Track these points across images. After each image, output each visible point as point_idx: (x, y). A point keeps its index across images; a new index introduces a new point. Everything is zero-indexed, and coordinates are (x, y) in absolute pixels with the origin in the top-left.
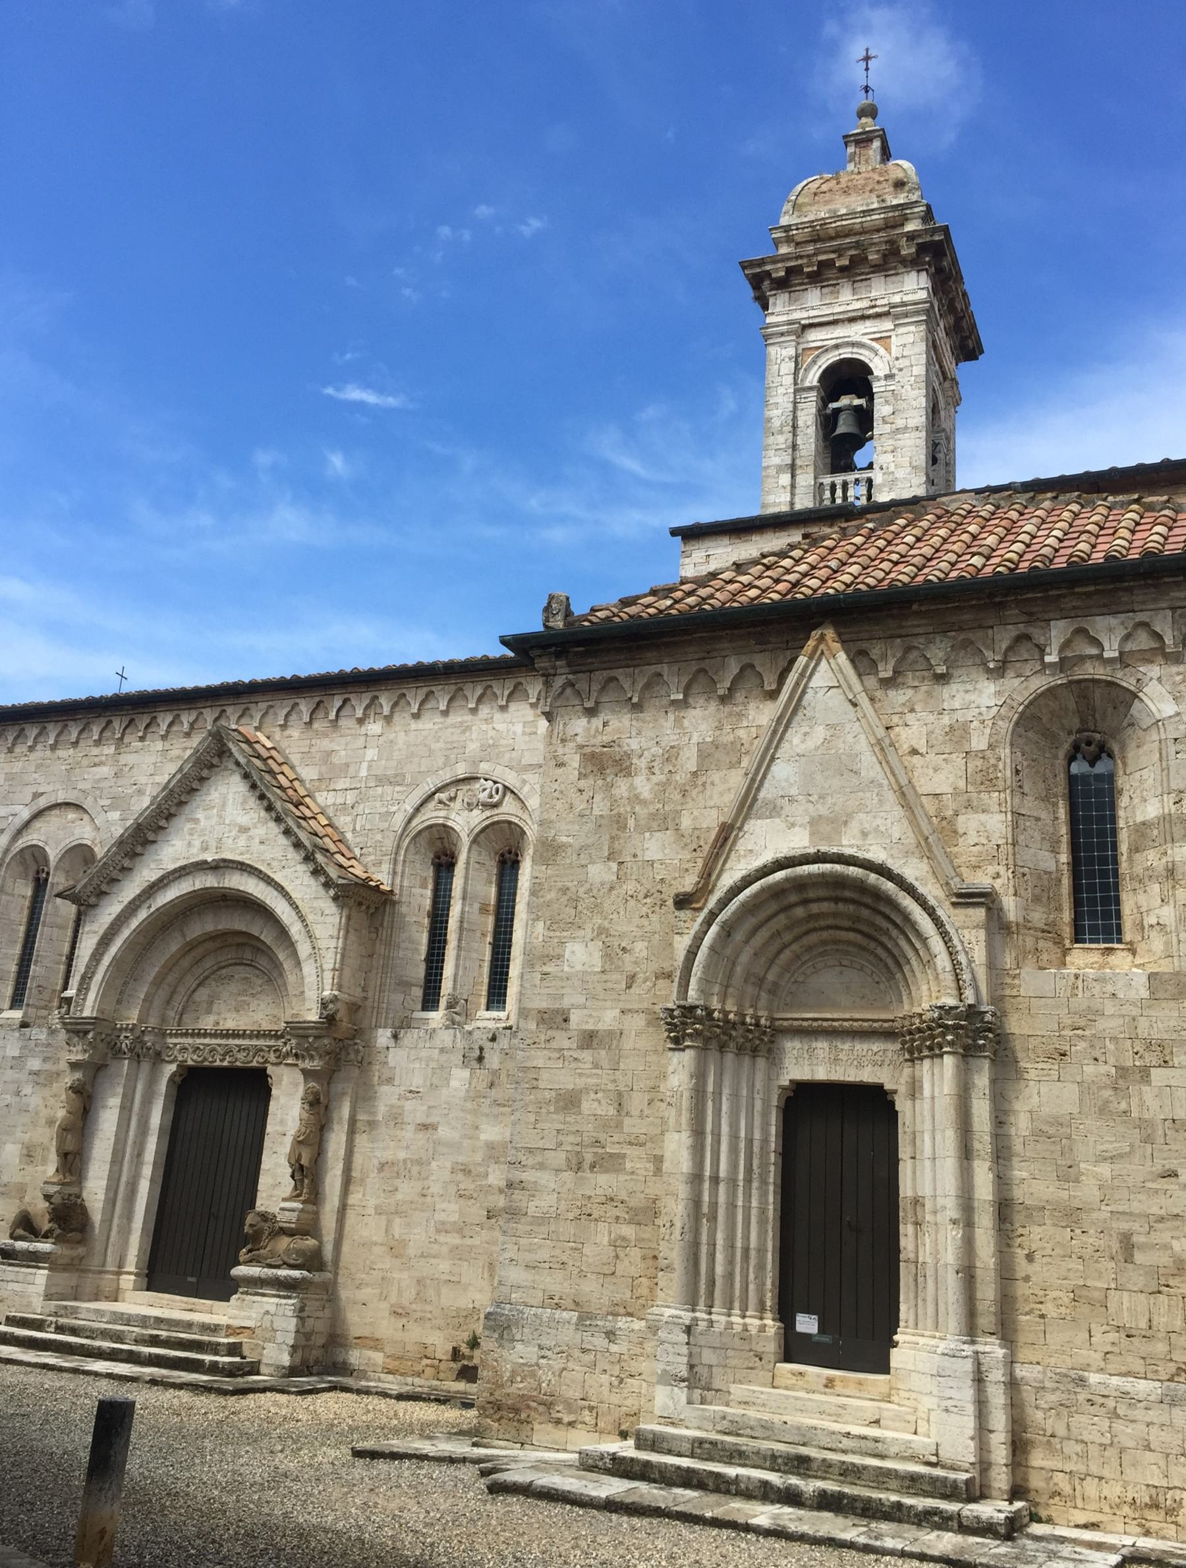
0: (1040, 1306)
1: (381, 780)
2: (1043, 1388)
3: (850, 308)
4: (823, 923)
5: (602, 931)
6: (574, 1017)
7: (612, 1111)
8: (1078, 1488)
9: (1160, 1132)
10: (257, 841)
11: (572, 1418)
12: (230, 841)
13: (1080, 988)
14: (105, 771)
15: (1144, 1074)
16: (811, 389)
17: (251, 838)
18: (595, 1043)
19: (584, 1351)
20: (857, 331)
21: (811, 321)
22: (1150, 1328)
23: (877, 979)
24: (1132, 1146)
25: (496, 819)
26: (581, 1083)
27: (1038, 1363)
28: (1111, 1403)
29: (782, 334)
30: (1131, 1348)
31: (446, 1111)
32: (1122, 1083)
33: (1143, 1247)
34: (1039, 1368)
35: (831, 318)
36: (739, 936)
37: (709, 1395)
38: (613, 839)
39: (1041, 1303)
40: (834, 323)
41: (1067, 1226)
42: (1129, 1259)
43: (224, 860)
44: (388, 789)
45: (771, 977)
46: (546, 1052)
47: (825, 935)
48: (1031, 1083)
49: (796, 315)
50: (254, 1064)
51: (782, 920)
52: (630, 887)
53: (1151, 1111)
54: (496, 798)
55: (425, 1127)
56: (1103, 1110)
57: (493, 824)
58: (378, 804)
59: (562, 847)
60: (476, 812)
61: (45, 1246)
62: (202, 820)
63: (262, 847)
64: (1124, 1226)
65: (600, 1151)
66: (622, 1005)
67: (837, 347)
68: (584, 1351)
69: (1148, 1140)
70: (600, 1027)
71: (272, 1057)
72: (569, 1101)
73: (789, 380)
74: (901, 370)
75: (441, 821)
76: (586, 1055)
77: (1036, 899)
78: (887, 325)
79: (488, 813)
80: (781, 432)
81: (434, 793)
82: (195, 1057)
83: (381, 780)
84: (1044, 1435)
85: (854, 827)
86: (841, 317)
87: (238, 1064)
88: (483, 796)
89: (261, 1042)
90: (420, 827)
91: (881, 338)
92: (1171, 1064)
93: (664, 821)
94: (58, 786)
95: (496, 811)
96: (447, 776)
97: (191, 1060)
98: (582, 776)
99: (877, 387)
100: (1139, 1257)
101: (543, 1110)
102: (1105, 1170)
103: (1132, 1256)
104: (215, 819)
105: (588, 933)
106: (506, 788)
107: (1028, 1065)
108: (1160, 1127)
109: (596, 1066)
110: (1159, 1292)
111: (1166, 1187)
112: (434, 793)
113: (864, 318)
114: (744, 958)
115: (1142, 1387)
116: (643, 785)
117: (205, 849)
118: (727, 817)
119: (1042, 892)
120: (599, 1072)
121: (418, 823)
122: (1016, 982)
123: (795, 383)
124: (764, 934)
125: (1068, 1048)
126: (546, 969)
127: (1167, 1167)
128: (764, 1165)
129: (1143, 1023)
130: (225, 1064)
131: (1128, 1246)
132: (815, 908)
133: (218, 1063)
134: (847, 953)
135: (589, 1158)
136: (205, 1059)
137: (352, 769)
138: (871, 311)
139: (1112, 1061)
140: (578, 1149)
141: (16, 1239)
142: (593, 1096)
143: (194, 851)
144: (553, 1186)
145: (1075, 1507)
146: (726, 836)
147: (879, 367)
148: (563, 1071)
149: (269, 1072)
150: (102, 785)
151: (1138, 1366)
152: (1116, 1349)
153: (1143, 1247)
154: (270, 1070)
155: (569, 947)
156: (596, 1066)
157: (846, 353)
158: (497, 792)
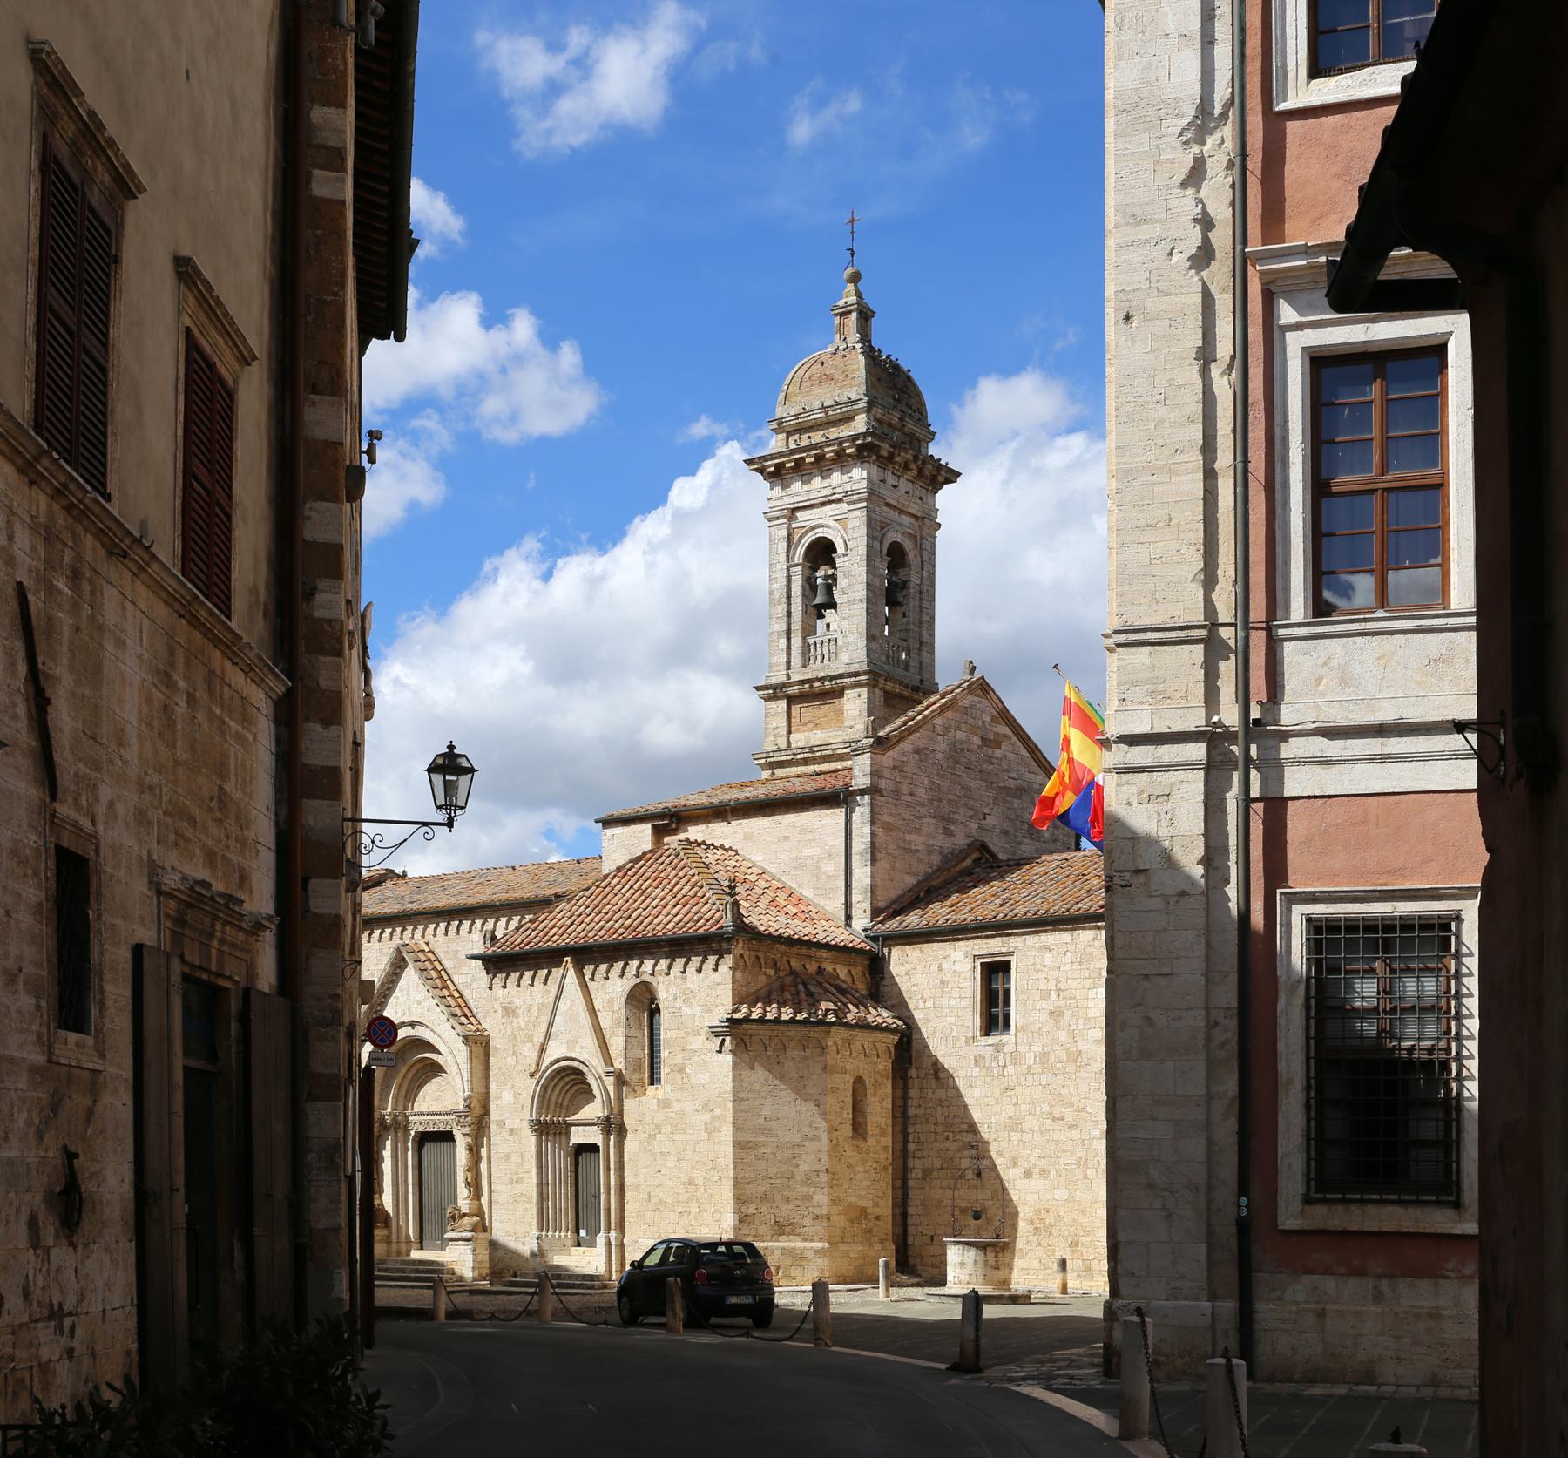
5: (513, 1086)
16: (797, 565)
20: (826, 514)
21: (797, 505)
29: (778, 518)
35: (808, 503)
36: (549, 1091)
38: (514, 1046)
40: (811, 507)
45: (565, 1104)
49: (787, 500)
51: (562, 1083)
52: (519, 1067)
56: (645, 1150)
67: (813, 528)
73: (783, 558)
76: (510, 1138)
77: (635, 1070)
80: (779, 603)
85: (578, 1046)
93: (529, 1038)
98: (503, 1017)
99: (839, 562)
102: (645, 1171)
105: (508, 1087)
114: (554, 1098)
116: (521, 1021)
118: (541, 1040)
119: (638, 1067)
123: (788, 562)
124: (558, 1088)
128: (566, 1177)
131: (650, 1197)
146: (543, 1049)
155: (504, 1093)
157: (819, 533)
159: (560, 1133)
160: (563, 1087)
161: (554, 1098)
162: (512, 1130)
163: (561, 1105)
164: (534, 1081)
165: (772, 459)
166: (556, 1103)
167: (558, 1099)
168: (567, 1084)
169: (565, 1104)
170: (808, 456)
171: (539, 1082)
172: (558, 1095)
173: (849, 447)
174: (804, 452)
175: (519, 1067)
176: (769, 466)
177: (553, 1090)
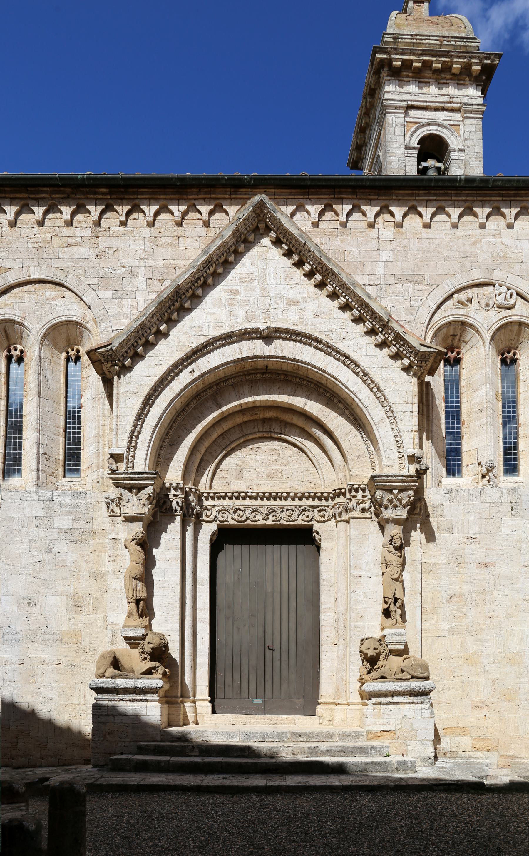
1: (399, 280)
3: (437, 99)
10: (310, 314)
12: (279, 312)
14: (83, 251)
25: (511, 319)
31: (501, 552)
43: (277, 330)
44: (408, 287)
50: (299, 522)
54: (512, 302)
55: (485, 565)
57: (507, 324)
58: (401, 300)
60: (492, 312)
62: (242, 292)
63: (316, 319)
71: (316, 515)
74: (468, 147)
75: (461, 318)
78: (458, 116)
79: (505, 313)
81: (452, 295)
82: (235, 516)
83: (399, 280)
86: (431, 104)
87: (282, 522)
88: (500, 299)
89: (304, 503)
90: (442, 322)
91: (453, 125)
94: (27, 263)
95: (510, 312)
96: (465, 281)
97: (230, 519)
104: (257, 291)
106: (518, 294)
112: (452, 295)
113: (444, 109)
117: (251, 319)
121: (441, 319)
130: (269, 522)
133: (261, 522)
136: (248, 519)
137: (368, 269)
138: (450, 105)
143: (240, 320)
147: (453, 142)
149: (315, 529)
150: (84, 264)
154: (317, 527)
158: (511, 296)
165: (402, 54)
170: (437, 61)
173: (477, 64)
174: (433, 56)
176: (396, 60)
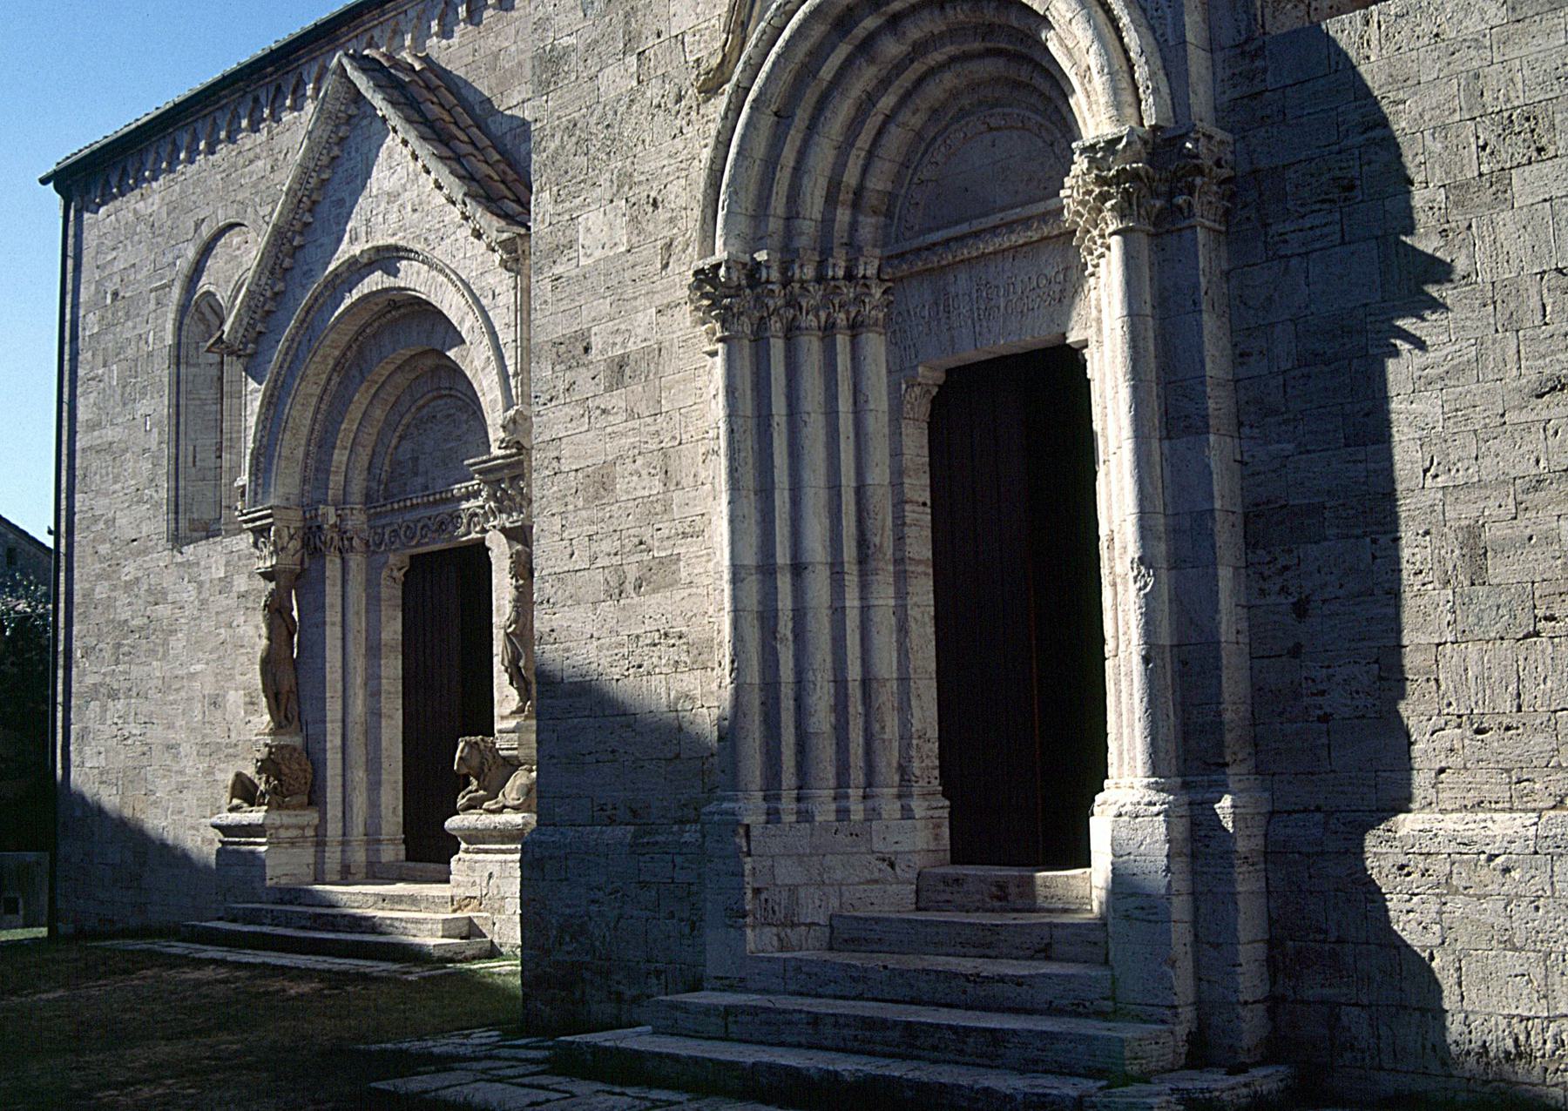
0: (1320, 700)
2: (1323, 853)
4: (937, 57)
5: (625, 180)
6: (596, 343)
7: (657, 486)
8: (1383, 1031)
9: (1534, 302)
11: (635, 992)
13: (1374, 43)
15: (1499, 181)
17: (403, 206)
18: (627, 380)
19: (644, 885)
22: (1519, 709)
23: (1048, 138)
24: (1479, 342)
26: (612, 448)
27: (1318, 809)
28: (1440, 867)
30: (1483, 754)
32: (1458, 218)
33: (1501, 548)
34: (1319, 816)
37: (793, 935)
39: (1322, 693)
41: (1365, 534)
42: (1477, 577)
46: (566, 409)
47: (949, 79)
48: (1294, 261)
53: (1515, 264)
59: (567, 51)
61: (256, 816)
64: (1462, 512)
65: (646, 557)
66: (660, 300)
68: (644, 885)
69: (1513, 324)
70: (631, 347)
72: (601, 483)
76: (617, 400)
84: (1324, 941)
92: (1551, 151)
100: (1497, 570)
101: (571, 507)
103: (1483, 569)
107: (1289, 227)
108: (1533, 291)
109: (632, 414)
110: (1537, 634)
111: (1545, 415)
114: (822, 157)
115: (1504, 826)
120: (635, 423)
122: (1259, 63)
125: (1355, 172)
126: (558, 270)
127: (1547, 371)
129: (1493, 78)
132: (915, 31)
134: (997, 103)
135: (632, 573)
139: (1438, 175)
140: (616, 560)
141: (232, 810)
142: (630, 467)
144: (589, 629)
145: (1381, 1068)
148: (590, 435)
151: (1497, 788)
152: (1453, 761)
153: (1501, 548)
156: (632, 414)
159: (855, 327)
160: (868, 102)
161: (822, 157)
162: (620, 365)
163: (859, 192)
164: (720, 103)
166: (834, 186)
167: (840, 166)
168: (884, 84)
169: (878, 183)
171: (742, 91)
172: (844, 150)
175: (653, 91)
177: (812, 128)
